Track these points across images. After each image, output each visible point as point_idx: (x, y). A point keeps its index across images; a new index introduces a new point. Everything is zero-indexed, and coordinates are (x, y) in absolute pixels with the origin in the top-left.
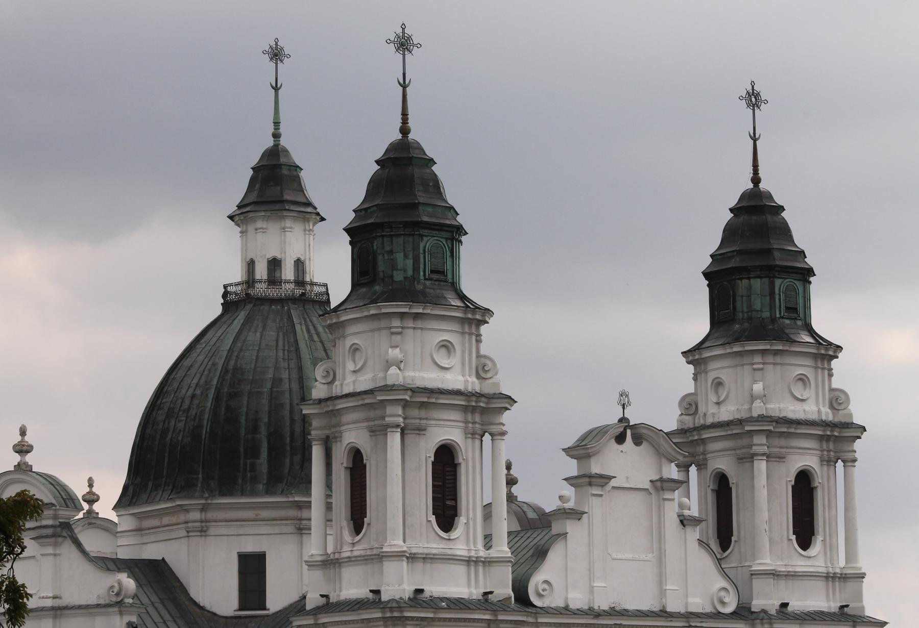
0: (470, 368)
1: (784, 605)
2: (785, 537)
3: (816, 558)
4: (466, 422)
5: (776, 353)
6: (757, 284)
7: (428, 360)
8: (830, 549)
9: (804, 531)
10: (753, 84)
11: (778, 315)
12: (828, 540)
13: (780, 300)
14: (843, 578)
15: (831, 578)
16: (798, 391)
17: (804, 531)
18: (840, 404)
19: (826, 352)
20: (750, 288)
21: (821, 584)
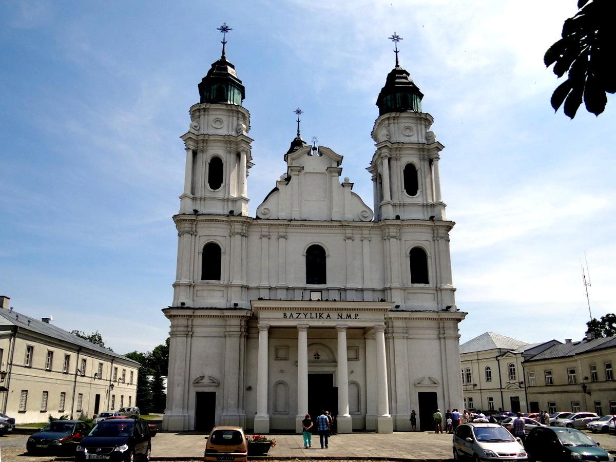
0: (232, 129)
1: (398, 217)
2: (400, 190)
3: (418, 199)
4: (227, 148)
5: (394, 118)
6: (389, 97)
7: (211, 127)
8: (424, 194)
9: (411, 186)
10: (395, 33)
11: (398, 106)
12: (424, 191)
13: (399, 101)
14: (433, 206)
15: (425, 206)
16: (408, 132)
17: (411, 186)
18: (431, 137)
19: (427, 120)
20: (386, 100)
21: (420, 209)
